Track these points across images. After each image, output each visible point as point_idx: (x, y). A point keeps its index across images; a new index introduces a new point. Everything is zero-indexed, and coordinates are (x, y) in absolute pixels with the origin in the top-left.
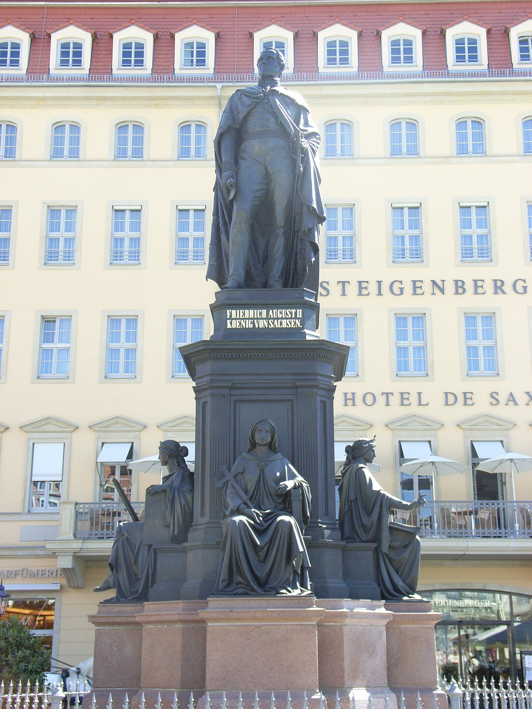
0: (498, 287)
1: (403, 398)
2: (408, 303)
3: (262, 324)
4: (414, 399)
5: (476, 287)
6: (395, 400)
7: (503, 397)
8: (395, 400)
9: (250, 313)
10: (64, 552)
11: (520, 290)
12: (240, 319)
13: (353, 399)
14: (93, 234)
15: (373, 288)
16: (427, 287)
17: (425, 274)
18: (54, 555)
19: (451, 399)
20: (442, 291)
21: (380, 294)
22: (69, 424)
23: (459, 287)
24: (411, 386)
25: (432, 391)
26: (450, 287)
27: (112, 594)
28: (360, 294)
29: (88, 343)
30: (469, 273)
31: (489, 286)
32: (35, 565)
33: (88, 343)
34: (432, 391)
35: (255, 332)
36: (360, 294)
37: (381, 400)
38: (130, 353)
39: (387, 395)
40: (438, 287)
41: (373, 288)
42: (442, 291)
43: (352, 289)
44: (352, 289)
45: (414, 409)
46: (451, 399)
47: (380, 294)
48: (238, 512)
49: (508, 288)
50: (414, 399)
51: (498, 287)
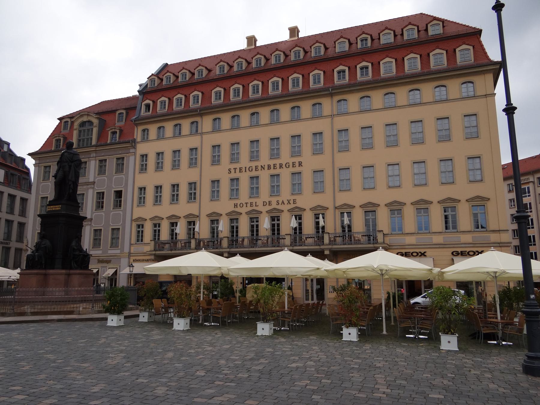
0: (281, 166)
1: (251, 204)
2: (254, 173)
4: (254, 204)
5: (274, 166)
6: (249, 205)
7: (280, 202)
8: (249, 205)
11: (287, 166)
15: (244, 170)
16: (260, 168)
17: (258, 164)
19: (265, 204)
20: (264, 169)
21: (246, 171)
23: (269, 167)
24: (253, 200)
25: (260, 202)
26: (266, 168)
30: (272, 163)
31: (278, 166)
34: (260, 202)
37: (245, 205)
38: (177, 195)
39: (246, 203)
40: (263, 168)
41: (244, 170)
42: (264, 169)
43: (238, 171)
44: (238, 171)
45: (254, 208)
46: (265, 204)
47: (246, 171)
49: (284, 166)
50: (254, 204)
51: (281, 166)
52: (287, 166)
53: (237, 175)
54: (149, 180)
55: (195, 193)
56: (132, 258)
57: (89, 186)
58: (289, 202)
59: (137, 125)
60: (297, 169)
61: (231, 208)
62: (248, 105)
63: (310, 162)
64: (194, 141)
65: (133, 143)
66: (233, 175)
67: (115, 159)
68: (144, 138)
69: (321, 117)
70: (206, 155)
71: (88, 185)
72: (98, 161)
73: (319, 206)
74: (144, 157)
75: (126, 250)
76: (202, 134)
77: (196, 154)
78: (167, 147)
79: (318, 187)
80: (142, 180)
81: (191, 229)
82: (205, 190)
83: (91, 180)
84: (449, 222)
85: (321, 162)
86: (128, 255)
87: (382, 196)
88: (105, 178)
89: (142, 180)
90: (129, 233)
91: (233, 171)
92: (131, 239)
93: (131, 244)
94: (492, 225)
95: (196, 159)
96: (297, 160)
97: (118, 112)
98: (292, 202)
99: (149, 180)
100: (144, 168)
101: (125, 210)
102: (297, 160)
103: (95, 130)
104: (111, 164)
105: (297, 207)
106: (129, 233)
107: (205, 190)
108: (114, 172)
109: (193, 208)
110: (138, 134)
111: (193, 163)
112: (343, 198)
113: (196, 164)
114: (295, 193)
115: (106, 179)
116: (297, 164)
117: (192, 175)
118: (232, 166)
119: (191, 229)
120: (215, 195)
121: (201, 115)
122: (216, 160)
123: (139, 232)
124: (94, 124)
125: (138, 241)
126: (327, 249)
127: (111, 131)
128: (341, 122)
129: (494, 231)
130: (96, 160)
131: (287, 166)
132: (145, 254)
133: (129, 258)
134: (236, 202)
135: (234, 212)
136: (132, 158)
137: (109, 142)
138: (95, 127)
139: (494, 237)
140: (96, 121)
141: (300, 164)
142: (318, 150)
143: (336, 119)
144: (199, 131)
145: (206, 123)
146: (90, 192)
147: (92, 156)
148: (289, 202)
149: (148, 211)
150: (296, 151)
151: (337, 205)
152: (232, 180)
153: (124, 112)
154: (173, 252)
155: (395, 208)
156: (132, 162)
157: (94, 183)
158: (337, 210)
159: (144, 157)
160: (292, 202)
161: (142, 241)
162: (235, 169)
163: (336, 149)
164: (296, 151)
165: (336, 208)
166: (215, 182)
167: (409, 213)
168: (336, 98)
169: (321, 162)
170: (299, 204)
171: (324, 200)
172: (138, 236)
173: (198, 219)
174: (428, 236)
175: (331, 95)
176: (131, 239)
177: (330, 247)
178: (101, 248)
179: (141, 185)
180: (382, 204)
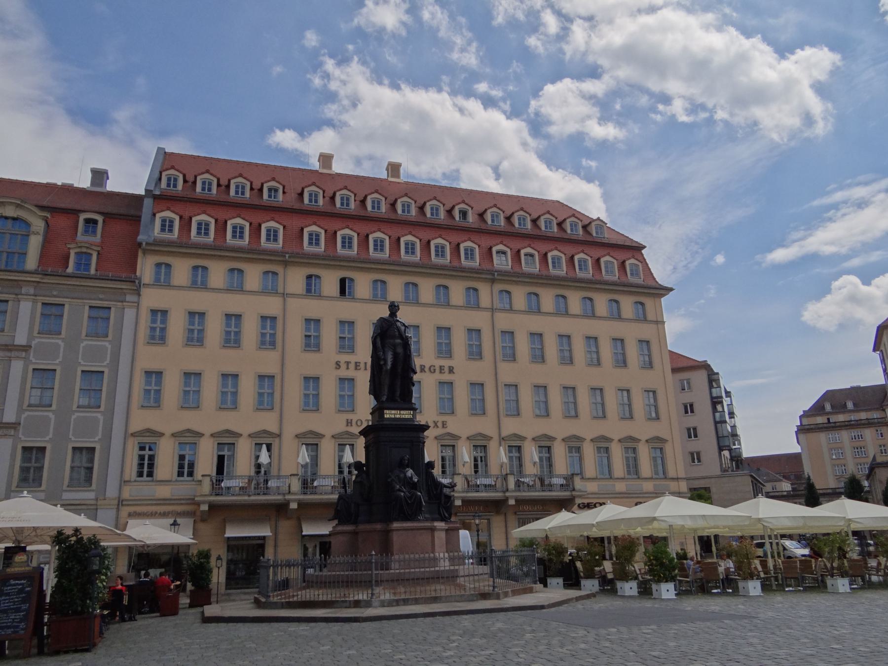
3: (398, 416)
9: (393, 412)
10: (204, 502)
12: (389, 414)
13: (351, 423)
14: (214, 328)
15: (362, 366)
18: (198, 504)
21: (366, 369)
22: (199, 433)
27: (336, 522)
28: (356, 369)
29: (210, 388)
32: (179, 509)
33: (210, 388)
35: (395, 419)
36: (356, 369)
43: (352, 366)
44: (352, 366)
48: (399, 490)
49: (427, 369)
52: (432, 369)
53: (351, 373)
54: (174, 357)
55: (271, 395)
56: (125, 510)
57: (13, 354)
58: (436, 423)
59: (145, 252)
60: (446, 377)
61: (341, 427)
62: (373, 266)
63: (465, 371)
64: (272, 306)
65: (136, 286)
66: (344, 373)
67: (87, 308)
68: (157, 280)
69: (477, 307)
70: (295, 333)
71: (10, 350)
72: (39, 305)
73: (480, 434)
74: (160, 314)
75: (112, 491)
76: (284, 295)
77: (273, 327)
78: (215, 305)
79: (478, 409)
80: (150, 357)
81: (144, 456)
82: (293, 392)
83: (21, 339)
84: (633, 467)
85: (481, 371)
86: (116, 502)
87: (558, 427)
88: (60, 342)
89: (150, 357)
90: (120, 459)
91: (343, 366)
92: (122, 472)
93: (124, 482)
94: (671, 473)
95: (273, 336)
96: (446, 363)
97: (83, 217)
98: (440, 424)
99: (174, 357)
100: (158, 337)
101: (110, 412)
102: (446, 363)
103: (35, 243)
104: (76, 313)
105: (449, 434)
106: (120, 459)
107: (293, 392)
108: (84, 333)
109: (268, 421)
110: (146, 268)
111: (268, 341)
112: (510, 426)
113: (273, 344)
114: (225, 406)
115: (62, 344)
116: (446, 370)
117: (269, 362)
118: (344, 358)
119: (144, 456)
120: (312, 403)
121: (286, 264)
122: (312, 343)
123: (142, 458)
124: (33, 229)
125: (140, 474)
126: (512, 497)
127: (78, 250)
128: (504, 321)
129: (673, 479)
130: (35, 302)
131: (432, 369)
132: (164, 501)
133: (118, 510)
134: (350, 416)
135: (347, 433)
136: (129, 314)
137: (70, 269)
138: (38, 233)
139: (673, 485)
140: (38, 225)
141: (451, 370)
142: (475, 353)
143: (499, 316)
144: (280, 290)
145: (295, 280)
146: (17, 366)
147: (24, 291)
148: (436, 423)
149: (169, 419)
150: (445, 350)
151: (504, 434)
152: (342, 380)
153: (100, 219)
154: (253, 498)
155: (574, 445)
156: (131, 320)
157: (26, 348)
158: (503, 443)
159: (160, 314)
160: (440, 424)
161: (150, 474)
162: (348, 363)
163: (499, 357)
164: (445, 350)
165: (502, 439)
166: (312, 381)
167: (589, 451)
168: (498, 287)
169: (481, 371)
170: (452, 428)
171: (486, 426)
172: (141, 465)
173: (277, 440)
174: (611, 483)
175: (493, 281)
176: (122, 472)
177: (518, 494)
178: (43, 487)
179: (154, 366)
180: (560, 437)
